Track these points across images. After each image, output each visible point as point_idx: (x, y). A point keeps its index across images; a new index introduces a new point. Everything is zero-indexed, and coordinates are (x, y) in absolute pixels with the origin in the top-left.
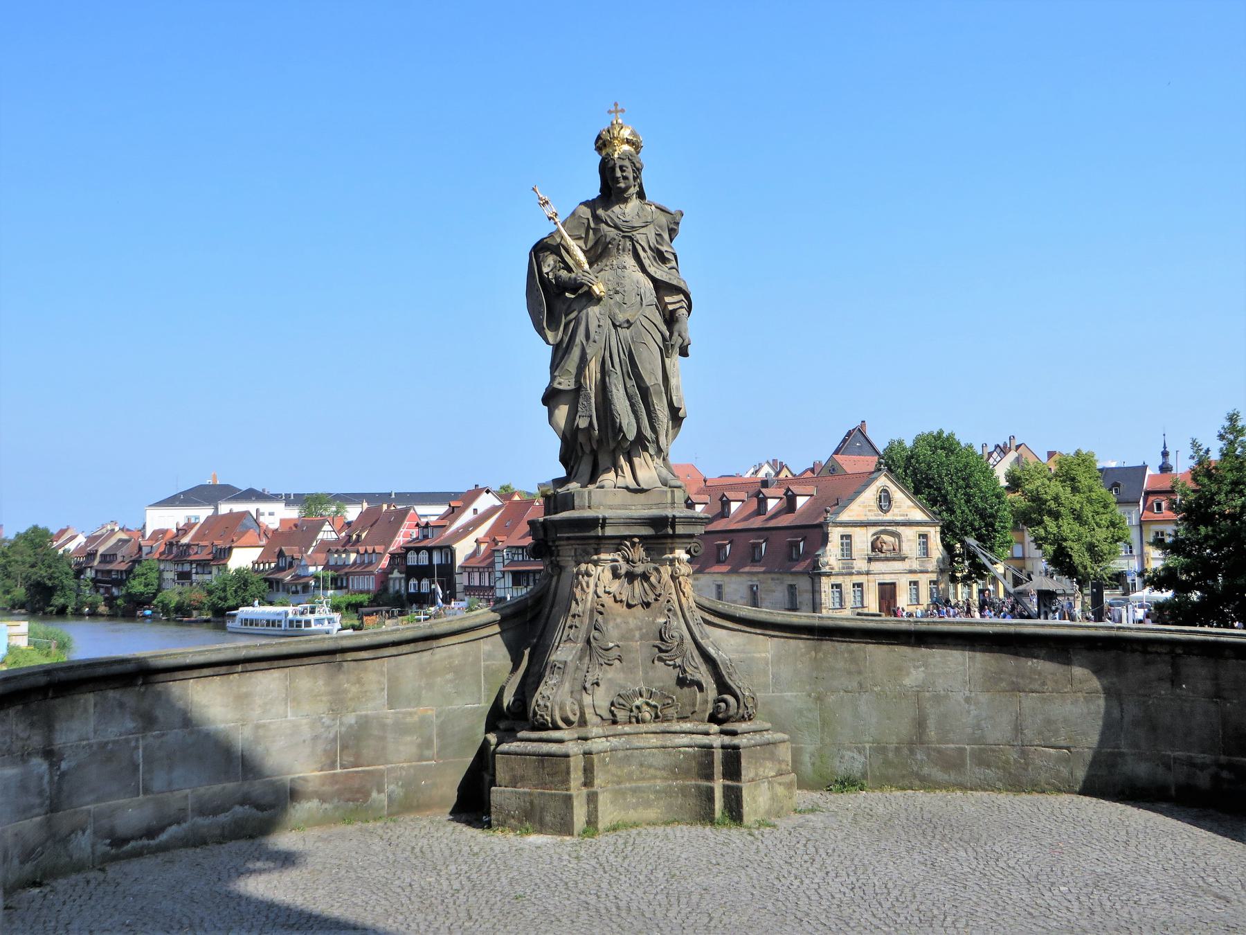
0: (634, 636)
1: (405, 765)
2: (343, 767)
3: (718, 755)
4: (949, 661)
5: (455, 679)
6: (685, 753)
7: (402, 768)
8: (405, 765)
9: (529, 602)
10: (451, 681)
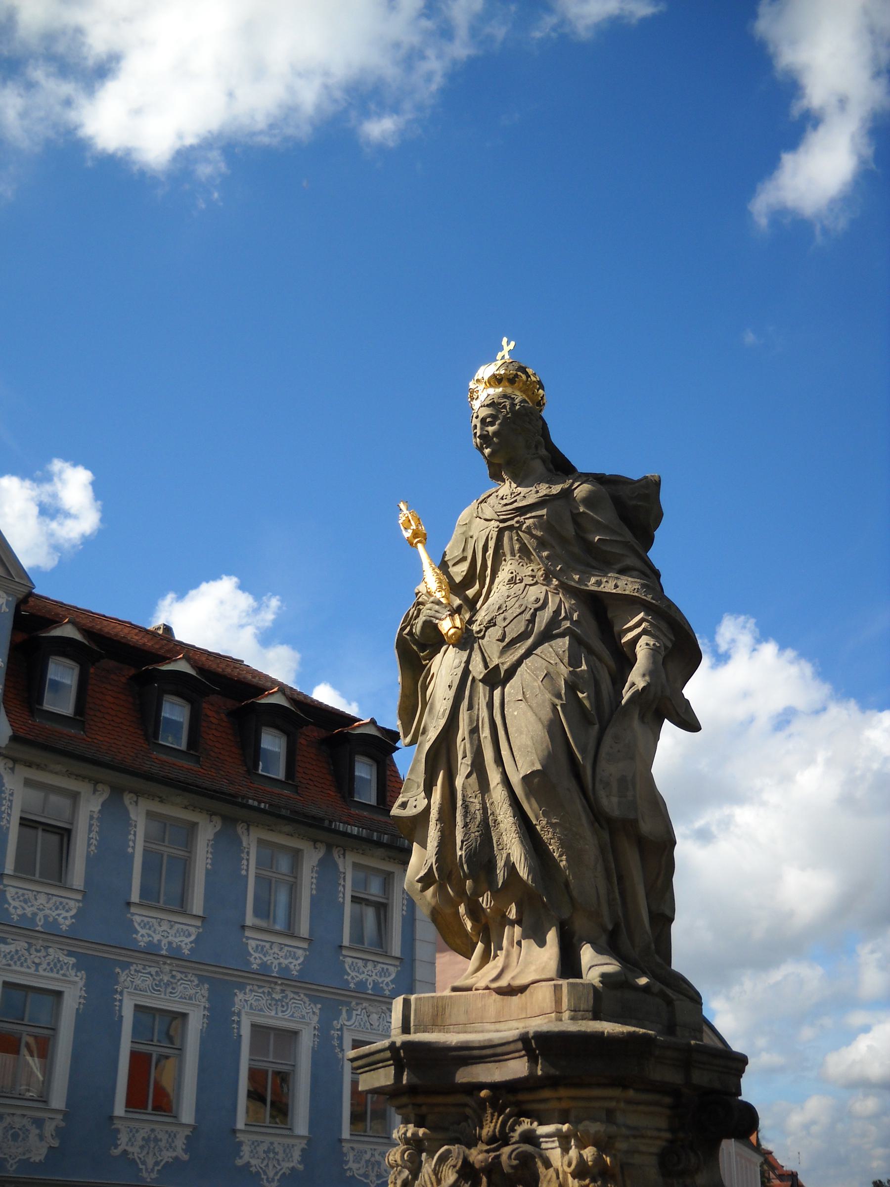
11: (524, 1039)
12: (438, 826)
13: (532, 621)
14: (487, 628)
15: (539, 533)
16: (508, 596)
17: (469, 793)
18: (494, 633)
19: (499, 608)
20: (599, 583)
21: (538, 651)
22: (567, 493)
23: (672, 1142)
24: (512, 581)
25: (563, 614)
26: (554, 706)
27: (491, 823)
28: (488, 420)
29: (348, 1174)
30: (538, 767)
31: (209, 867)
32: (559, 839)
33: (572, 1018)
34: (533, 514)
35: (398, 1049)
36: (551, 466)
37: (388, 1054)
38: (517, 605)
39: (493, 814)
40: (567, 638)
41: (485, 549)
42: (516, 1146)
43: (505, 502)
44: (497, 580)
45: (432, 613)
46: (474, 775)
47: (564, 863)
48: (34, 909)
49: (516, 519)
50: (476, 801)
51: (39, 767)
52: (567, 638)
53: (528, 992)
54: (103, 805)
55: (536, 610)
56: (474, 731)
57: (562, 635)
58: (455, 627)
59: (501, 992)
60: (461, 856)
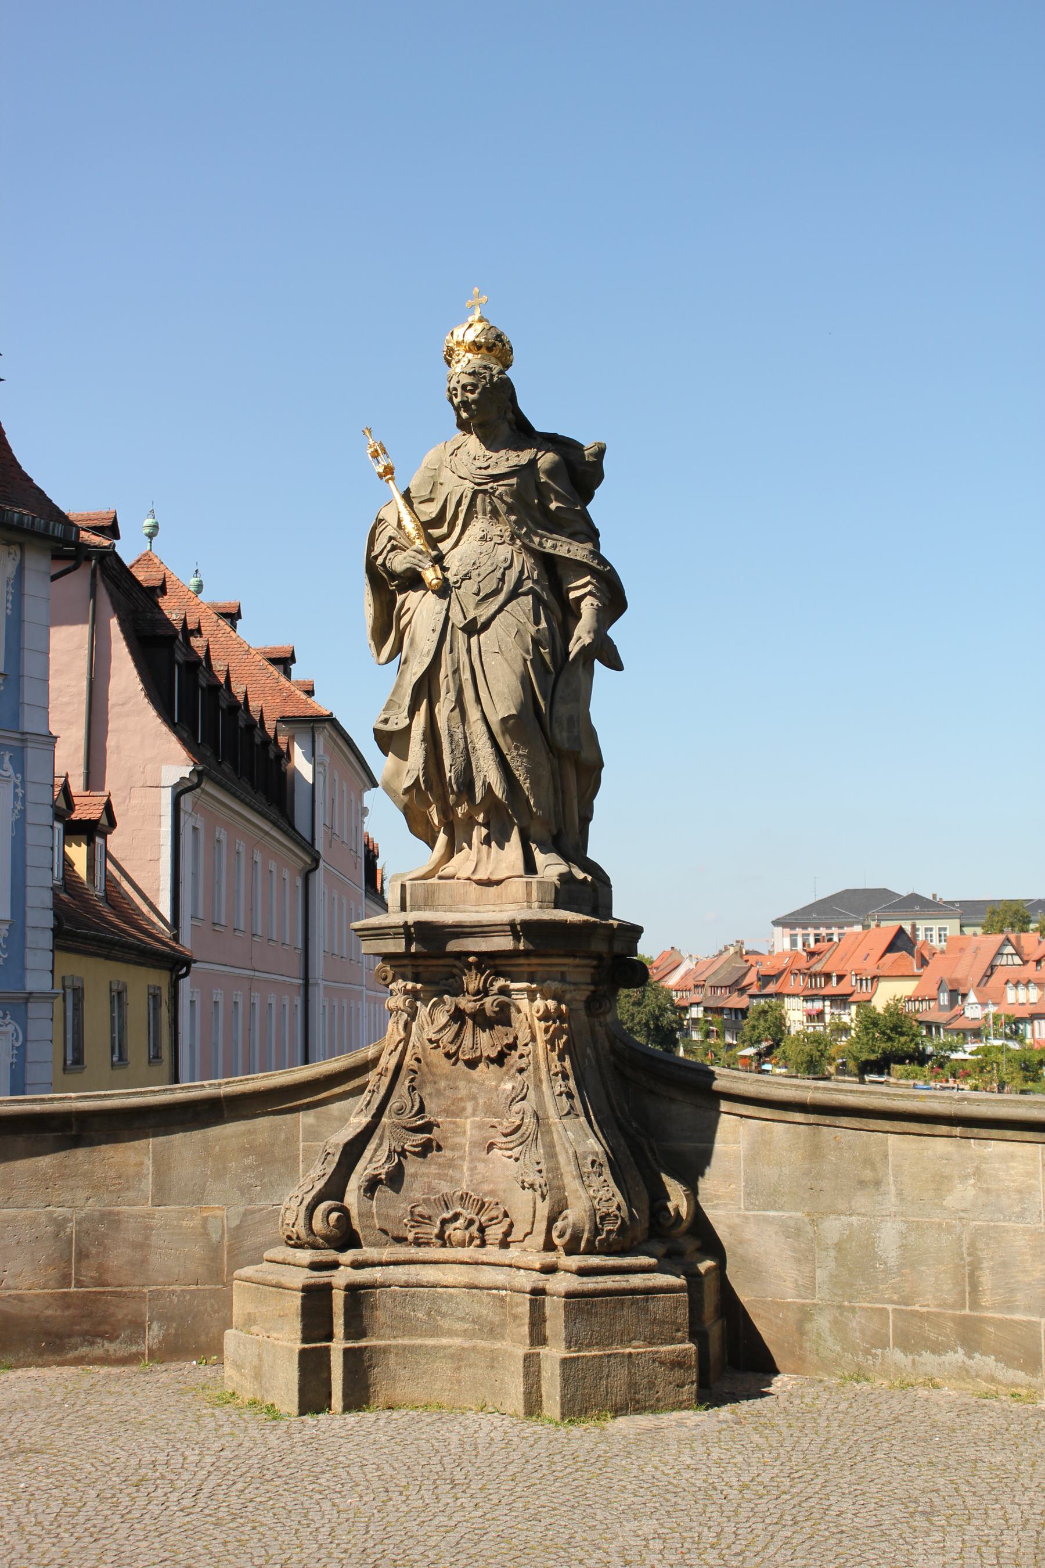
0: (464, 1109)
1: (177, 1288)
2: (79, 1284)
3: (338, 1299)
4: (1013, 1168)
5: (258, 1166)
6: (494, 1296)
7: (173, 1292)
8: (177, 1288)
9: (370, 1053)
10: (250, 1168)
11: (512, 925)
12: (423, 746)
13: (502, 579)
14: (463, 580)
15: (509, 500)
16: (481, 553)
17: (453, 724)
18: (469, 587)
19: (474, 564)
20: (554, 547)
21: (508, 608)
22: (533, 462)
23: (593, 992)
24: (483, 539)
25: (526, 574)
26: (525, 660)
27: (471, 750)
28: (469, 388)
30: (514, 712)
32: (526, 767)
33: (540, 907)
34: (505, 482)
35: (410, 926)
36: (515, 427)
37: (402, 930)
38: (489, 563)
39: (472, 742)
40: (530, 596)
41: (459, 503)
42: (496, 997)
43: (478, 464)
44: (467, 533)
45: (416, 561)
46: (457, 710)
47: (528, 785)
49: (491, 485)
50: (458, 731)
52: (530, 596)
53: (503, 884)
55: (505, 569)
56: (456, 671)
57: (526, 594)
58: (438, 578)
59: (481, 883)
60: (450, 777)
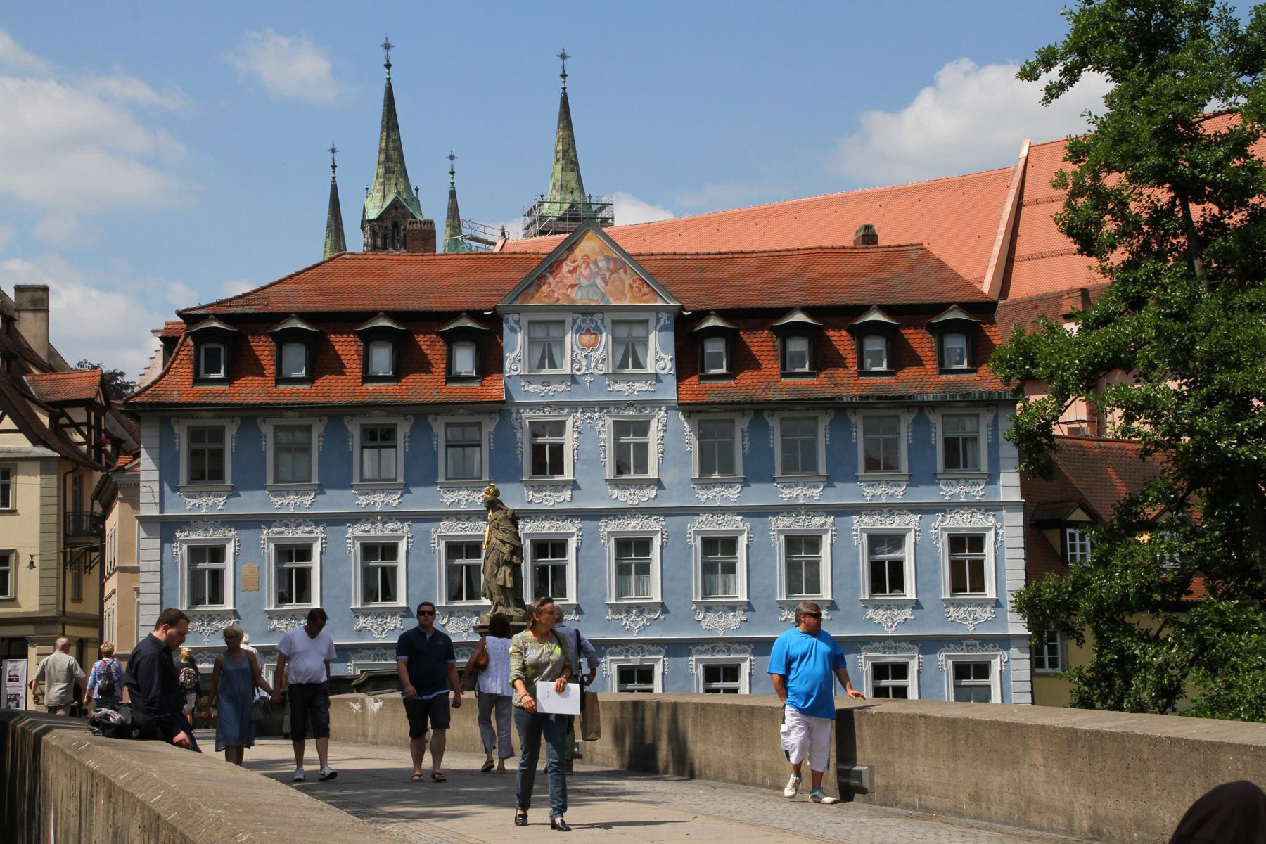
29: (950, 619)
31: (828, 443)
48: (714, 494)
51: (705, 412)
54: (750, 422)
